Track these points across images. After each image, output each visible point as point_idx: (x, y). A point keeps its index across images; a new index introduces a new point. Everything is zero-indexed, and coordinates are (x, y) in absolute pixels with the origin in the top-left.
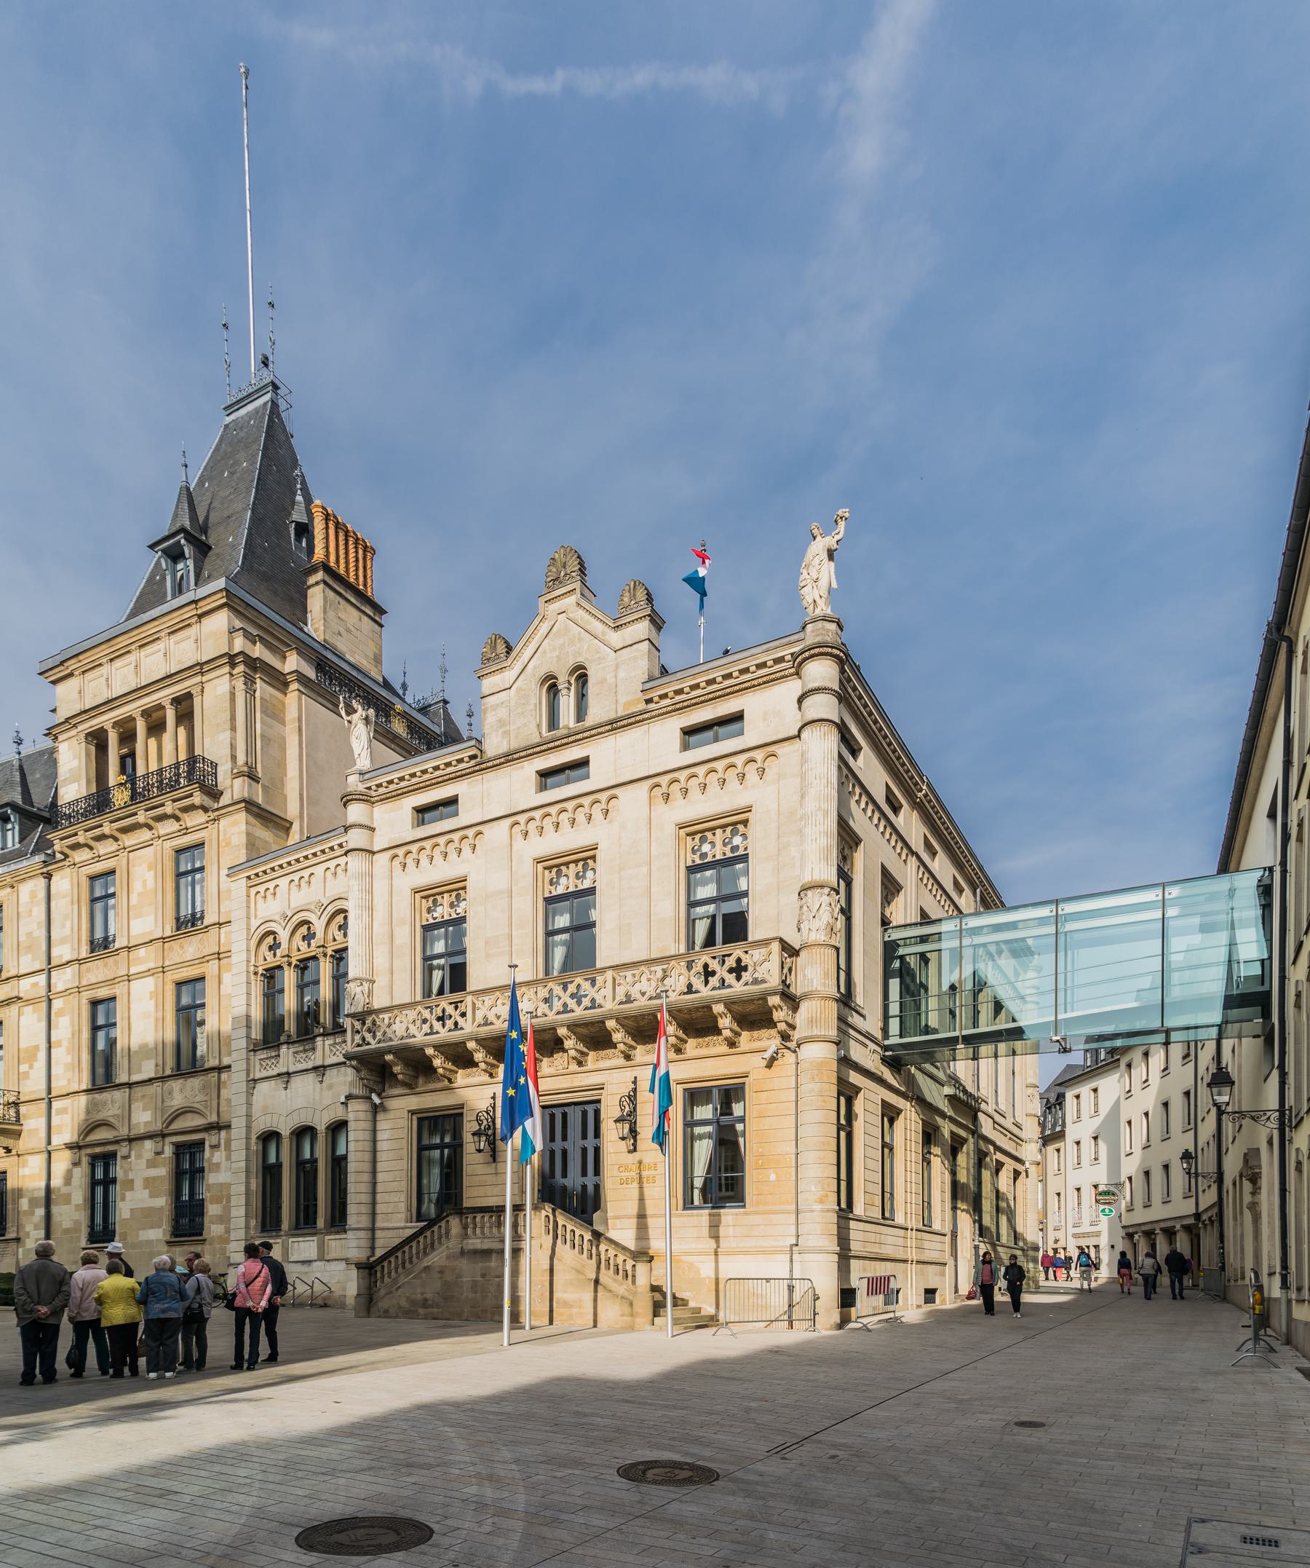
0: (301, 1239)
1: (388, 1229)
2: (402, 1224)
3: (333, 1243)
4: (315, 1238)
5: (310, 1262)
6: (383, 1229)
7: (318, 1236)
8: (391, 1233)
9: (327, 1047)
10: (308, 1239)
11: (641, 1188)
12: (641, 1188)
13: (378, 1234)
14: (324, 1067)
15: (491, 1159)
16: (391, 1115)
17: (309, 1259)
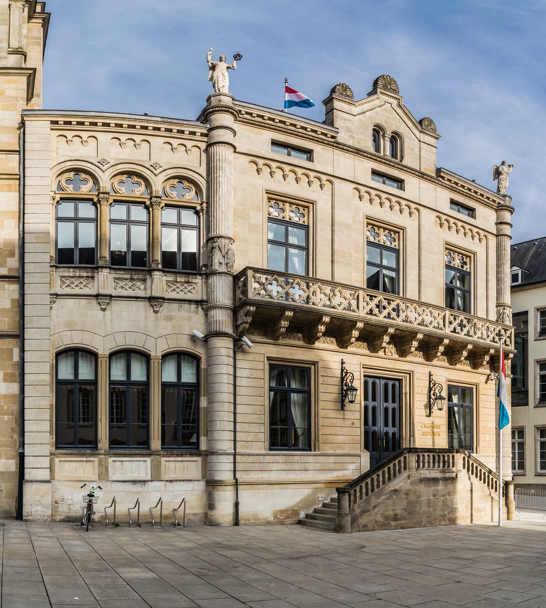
0: (127, 459)
1: (249, 455)
2: (263, 452)
3: (172, 465)
4: (148, 459)
5: (145, 482)
6: (243, 455)
7: (152, 457)
8: (251, 459)
9: (165, 282)
10: (135, 459)
11: (433, 439)
12: (433, 439)
13: (238, 458)
14: (163, 299)
15: (339, 406)
16: (250, 357)
17: (143, 479)
